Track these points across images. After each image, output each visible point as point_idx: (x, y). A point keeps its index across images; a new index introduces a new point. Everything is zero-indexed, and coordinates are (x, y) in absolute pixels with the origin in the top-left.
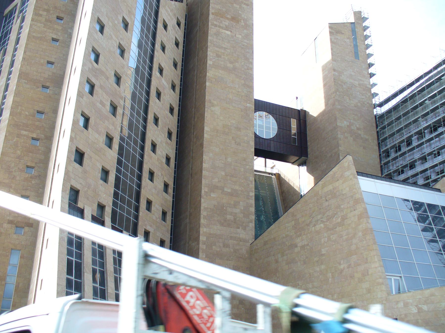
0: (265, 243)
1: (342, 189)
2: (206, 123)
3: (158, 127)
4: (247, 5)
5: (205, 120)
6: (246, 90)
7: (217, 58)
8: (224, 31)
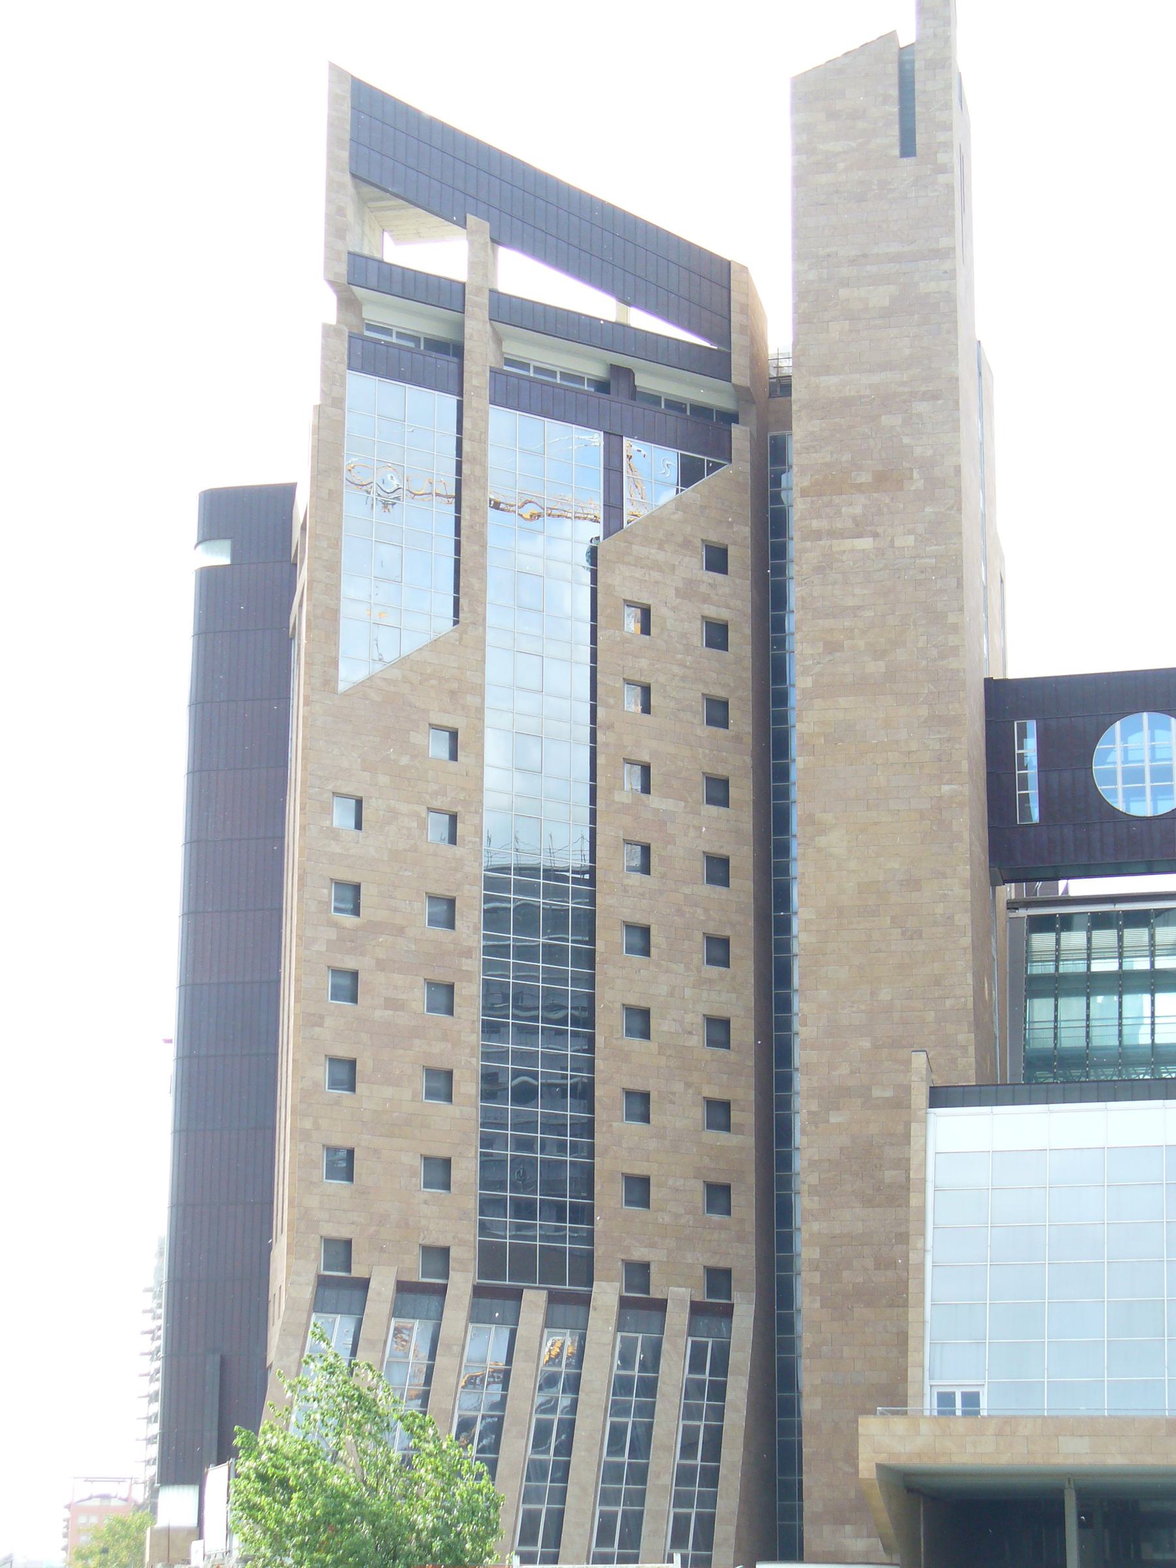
4: (935, 396)
6: (938, 736)
7: (829, 657)
8: (848, 544)
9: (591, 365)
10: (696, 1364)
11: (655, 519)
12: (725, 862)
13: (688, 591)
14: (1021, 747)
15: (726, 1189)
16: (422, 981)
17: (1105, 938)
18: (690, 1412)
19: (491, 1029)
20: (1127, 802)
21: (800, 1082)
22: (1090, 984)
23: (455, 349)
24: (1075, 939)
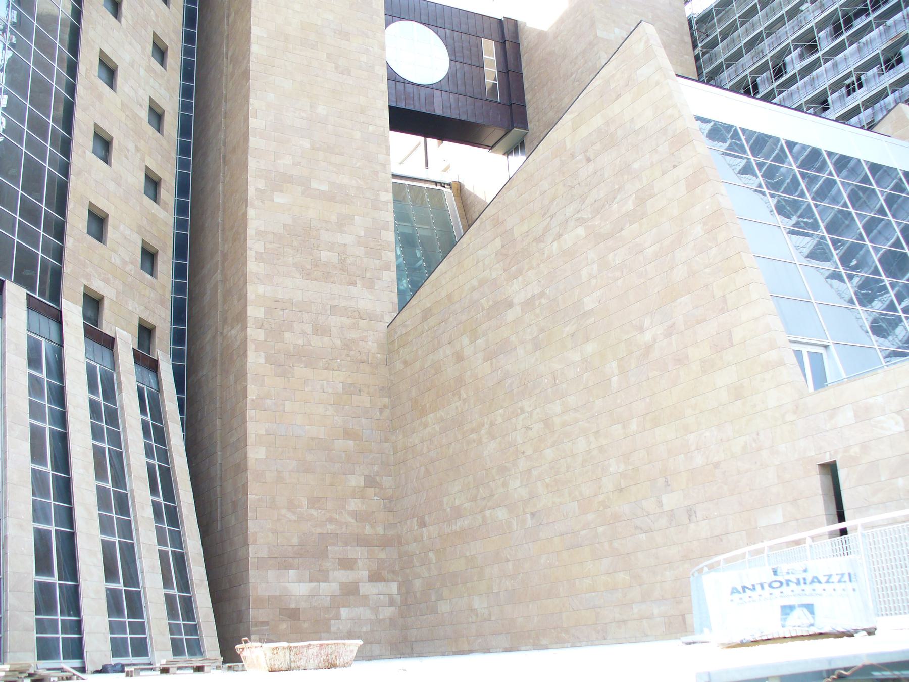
0: (427, 314)
1: (633, 118)
2: (255, 16)
3: (120, 21)
5: (253, 10)
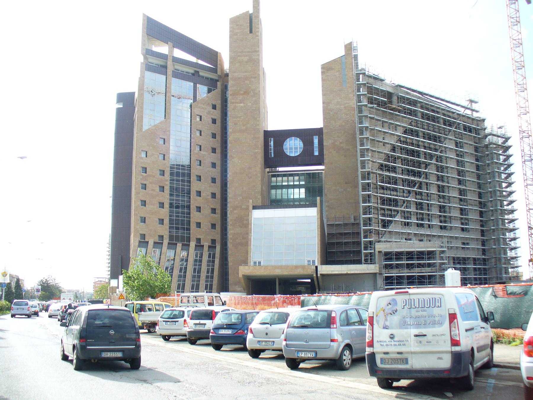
4: (255, 78)
9: (191, 70)
10: (209, 257)
11: (203, 99)
12: (215, 164)
13: (209, 113)
14: (270, 143)
15: (215, 225)
16: (158, 186)
17: (285, 178)
18: (208, 266)
19: (171, 195)
20: (289, 153)
21: (229, 205)
22: (282, 187)
23: (165, 67)
24: (280, 179)
